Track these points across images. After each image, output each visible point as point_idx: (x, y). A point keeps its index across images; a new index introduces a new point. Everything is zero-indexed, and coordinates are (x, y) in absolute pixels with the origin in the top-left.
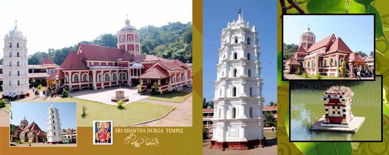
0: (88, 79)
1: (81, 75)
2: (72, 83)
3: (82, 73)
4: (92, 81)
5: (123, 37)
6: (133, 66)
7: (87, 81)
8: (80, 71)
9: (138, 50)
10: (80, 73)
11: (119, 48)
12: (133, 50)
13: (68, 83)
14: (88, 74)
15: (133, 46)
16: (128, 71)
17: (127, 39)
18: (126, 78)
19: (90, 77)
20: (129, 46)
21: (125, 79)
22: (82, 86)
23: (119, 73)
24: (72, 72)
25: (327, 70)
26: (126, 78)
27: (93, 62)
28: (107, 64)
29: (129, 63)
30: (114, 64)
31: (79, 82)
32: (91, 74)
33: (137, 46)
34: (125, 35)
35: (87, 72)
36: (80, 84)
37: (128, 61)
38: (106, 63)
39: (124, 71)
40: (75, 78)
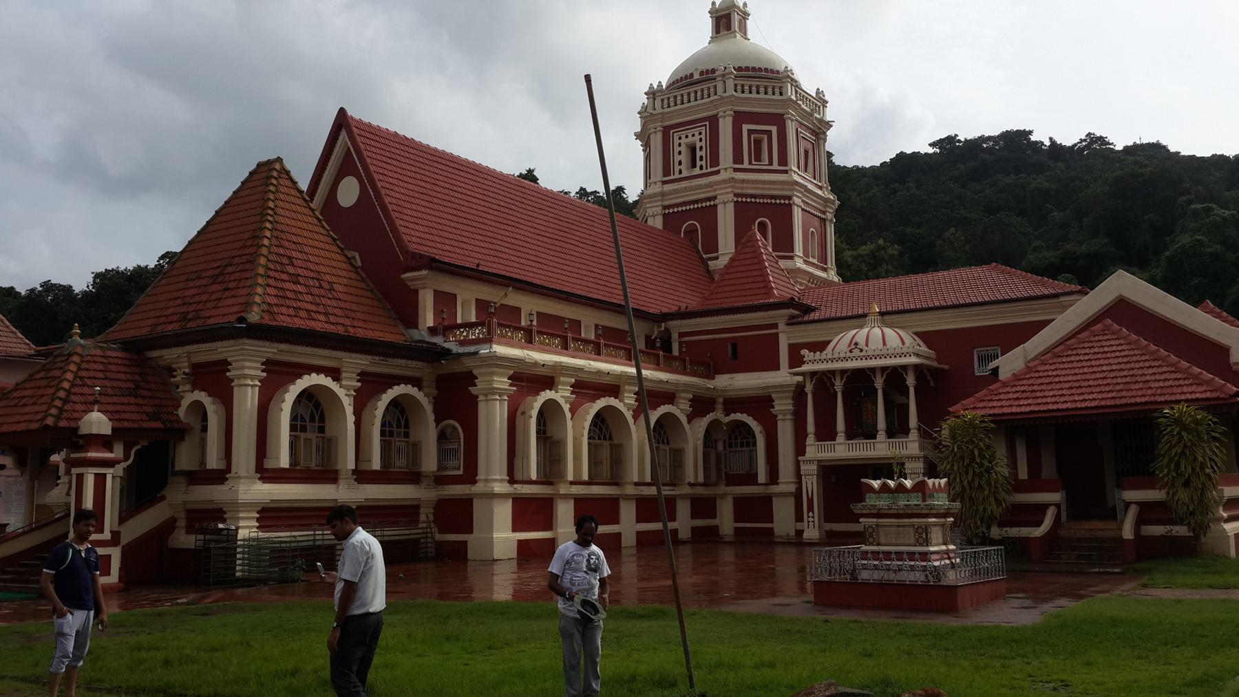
4: (470, 475)
5: (698, 136)
9: (823, 259)
11: (658, 223)
12: (784, 244)
13: (220, 476)
16: (783, 406)
17: (738, 158)
18: (762, 478)
19: (442, 437)
20: (747, 211)
21: (751, 479)
23: (703, 423)
24: (269, 365)
26: (762, 478)
27: (467, 297)
28: (588, 333)
31: (328, 475)
32: (457, 397)
34: (713, 121)
38: (576, 325)
39: (734, 403)
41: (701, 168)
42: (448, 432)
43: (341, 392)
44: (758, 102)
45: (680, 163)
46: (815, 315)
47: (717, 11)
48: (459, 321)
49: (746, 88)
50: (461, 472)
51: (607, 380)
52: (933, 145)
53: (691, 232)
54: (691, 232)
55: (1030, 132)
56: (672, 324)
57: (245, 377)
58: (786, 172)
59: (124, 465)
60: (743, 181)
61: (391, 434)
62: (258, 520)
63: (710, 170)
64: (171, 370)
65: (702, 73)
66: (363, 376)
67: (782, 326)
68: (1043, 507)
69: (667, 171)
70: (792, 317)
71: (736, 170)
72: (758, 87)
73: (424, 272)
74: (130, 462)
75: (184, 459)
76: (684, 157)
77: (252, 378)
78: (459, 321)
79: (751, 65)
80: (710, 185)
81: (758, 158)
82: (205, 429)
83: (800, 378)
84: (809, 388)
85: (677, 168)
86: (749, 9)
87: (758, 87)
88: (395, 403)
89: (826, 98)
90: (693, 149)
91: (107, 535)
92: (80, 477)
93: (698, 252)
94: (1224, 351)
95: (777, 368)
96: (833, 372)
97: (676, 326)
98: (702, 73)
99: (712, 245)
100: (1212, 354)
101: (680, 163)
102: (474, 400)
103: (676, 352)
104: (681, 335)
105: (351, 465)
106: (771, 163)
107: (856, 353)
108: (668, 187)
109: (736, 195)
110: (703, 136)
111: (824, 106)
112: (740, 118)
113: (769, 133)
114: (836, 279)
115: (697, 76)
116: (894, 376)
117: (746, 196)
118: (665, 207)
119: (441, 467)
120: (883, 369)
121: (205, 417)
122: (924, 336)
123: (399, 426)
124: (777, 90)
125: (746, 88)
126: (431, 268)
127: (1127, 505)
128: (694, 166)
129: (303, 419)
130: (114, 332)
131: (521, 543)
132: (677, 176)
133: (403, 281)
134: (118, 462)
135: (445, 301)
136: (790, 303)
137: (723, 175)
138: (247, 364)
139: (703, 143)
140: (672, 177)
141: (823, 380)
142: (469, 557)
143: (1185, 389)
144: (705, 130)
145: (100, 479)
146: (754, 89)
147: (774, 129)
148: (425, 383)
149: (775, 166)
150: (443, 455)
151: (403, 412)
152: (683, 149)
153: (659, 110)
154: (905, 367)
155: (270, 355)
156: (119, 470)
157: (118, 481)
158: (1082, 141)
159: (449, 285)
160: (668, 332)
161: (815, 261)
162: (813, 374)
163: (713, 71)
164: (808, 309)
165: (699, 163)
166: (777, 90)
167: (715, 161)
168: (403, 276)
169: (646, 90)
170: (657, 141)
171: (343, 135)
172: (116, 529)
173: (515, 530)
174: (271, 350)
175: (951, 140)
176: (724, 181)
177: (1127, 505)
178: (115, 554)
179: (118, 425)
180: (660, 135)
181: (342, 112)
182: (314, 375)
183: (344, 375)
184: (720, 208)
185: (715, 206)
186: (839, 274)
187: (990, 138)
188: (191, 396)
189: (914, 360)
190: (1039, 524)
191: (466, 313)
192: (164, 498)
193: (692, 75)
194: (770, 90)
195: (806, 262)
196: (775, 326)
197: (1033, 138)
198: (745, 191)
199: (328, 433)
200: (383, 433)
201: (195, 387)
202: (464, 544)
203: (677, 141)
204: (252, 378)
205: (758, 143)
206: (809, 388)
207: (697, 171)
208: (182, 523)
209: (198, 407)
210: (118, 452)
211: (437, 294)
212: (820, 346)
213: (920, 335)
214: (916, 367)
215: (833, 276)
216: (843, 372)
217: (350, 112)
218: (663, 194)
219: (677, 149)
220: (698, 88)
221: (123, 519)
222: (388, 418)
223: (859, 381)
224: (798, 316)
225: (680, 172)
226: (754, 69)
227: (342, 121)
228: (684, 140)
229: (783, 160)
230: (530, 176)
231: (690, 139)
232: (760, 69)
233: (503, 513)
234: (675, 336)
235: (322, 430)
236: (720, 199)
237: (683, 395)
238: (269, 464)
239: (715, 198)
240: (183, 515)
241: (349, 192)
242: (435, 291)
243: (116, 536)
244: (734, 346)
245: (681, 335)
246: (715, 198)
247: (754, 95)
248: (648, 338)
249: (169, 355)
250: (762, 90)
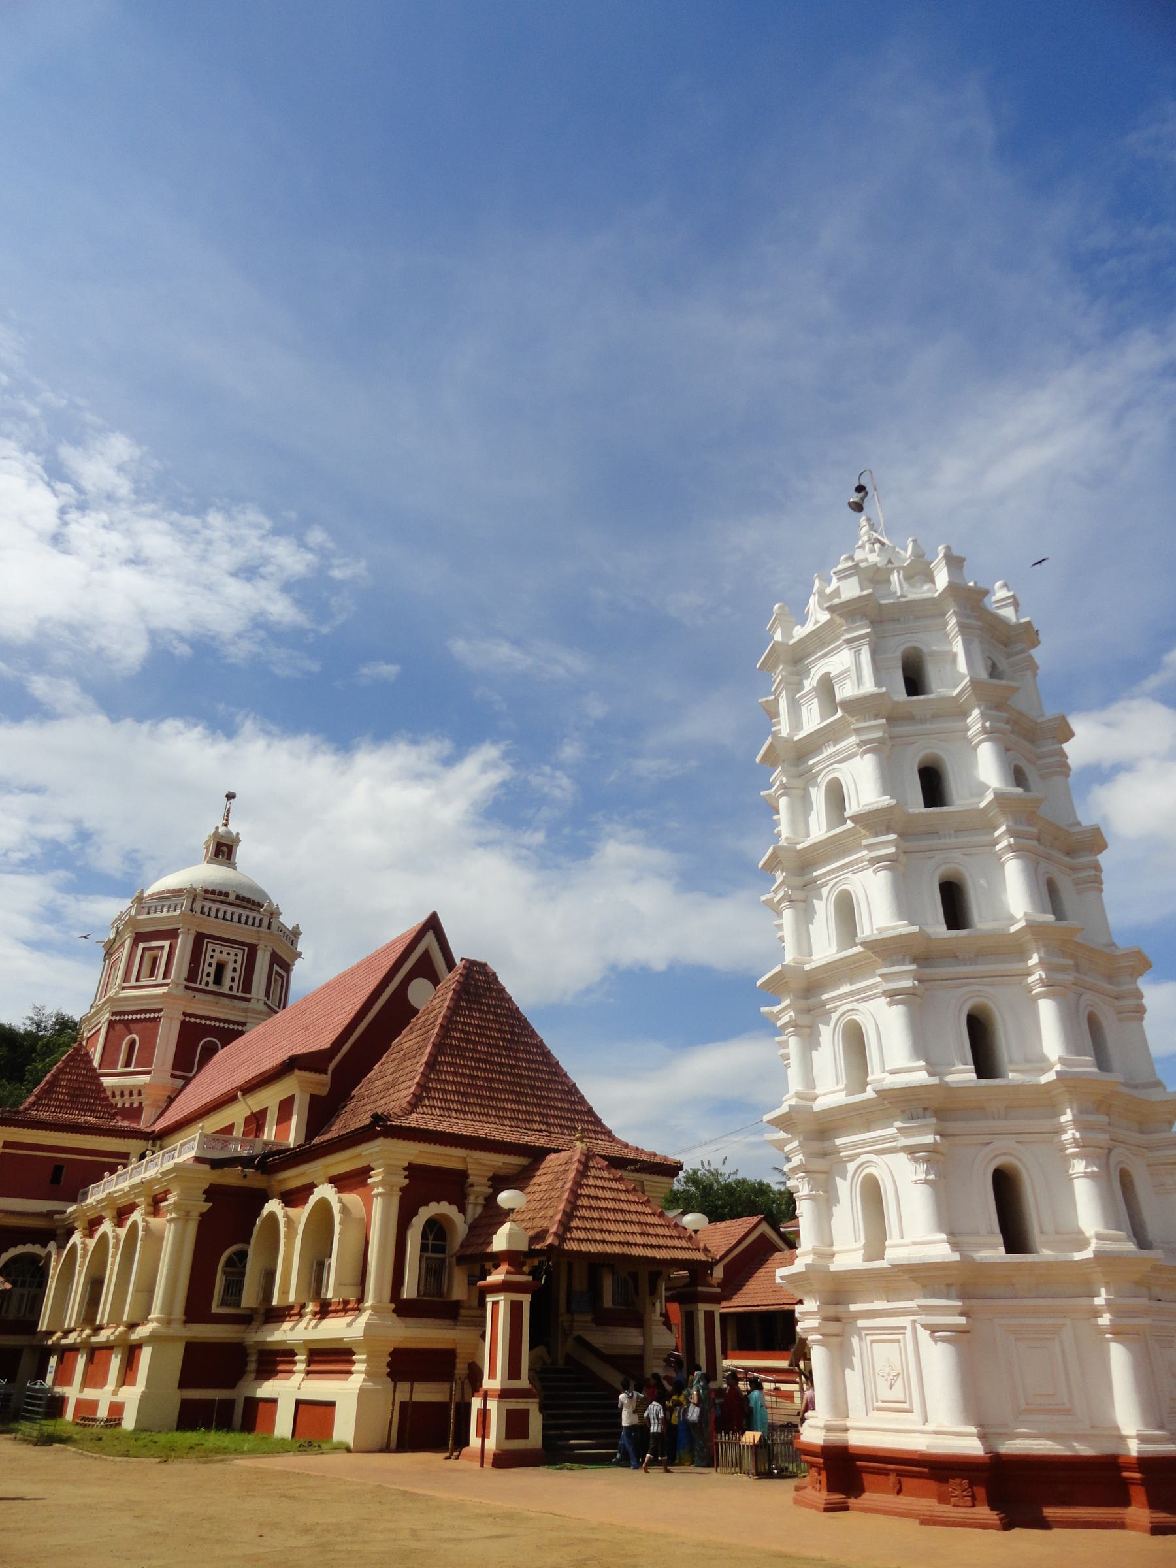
5: (233, 960)
25: (274, 1361)
41: (231, 988)
45: (209, 975)
63: (240, 994)
85: (205, 979)
90: (220, 968)
98: (238, 897)
110: (239, 959)
115: (232, 898)
118: (185, 1014)
132: (203, 987)
140: (197, 986)
165: (227, 982)
193: (227, 894)
203: (209, 953)
219: (208, 960)
220: (230, 909)
225: (207, 984)
231: (224, 957)
246: (244, 1024)
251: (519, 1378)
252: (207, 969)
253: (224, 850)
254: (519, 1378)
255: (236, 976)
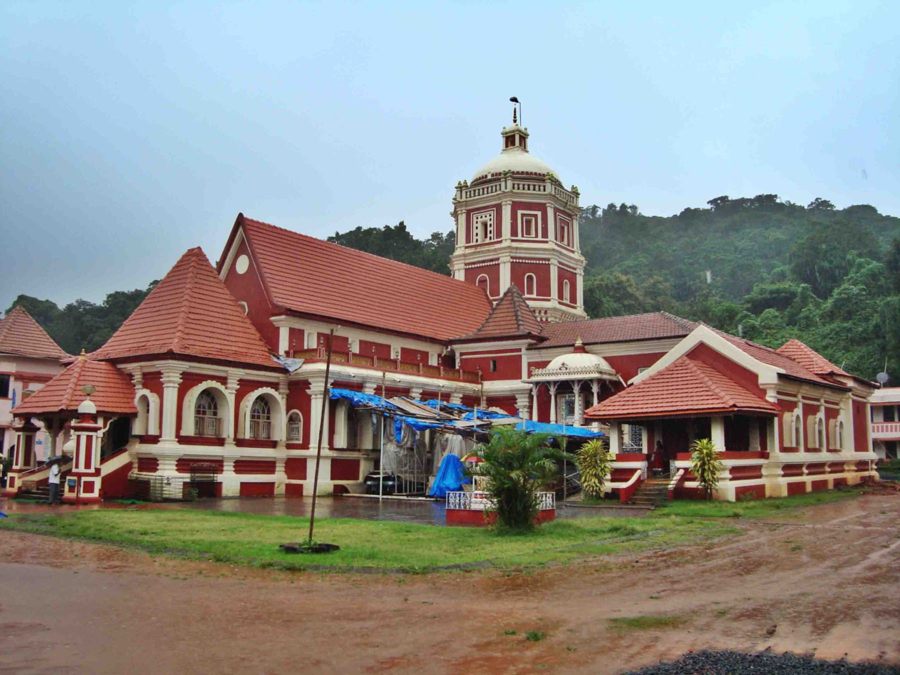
0: (280, 431)
1: (240, 396)
2: (183, 440)
3: (246, 386)
4: (305, 445)
5: (489, 217)
6: (550, 366)
7: (274, 445)
8: (235, 375)
9: (573, 299)
10: (234, 385)
11: (460, 276)
12: (544, 291)
13: (155, 440)
14: (280, 398)
15: (542, 269)
17: (514, 232)
19: (292, 420)
22: (242, 466)
24: (185, 375)
29: (526, 358)
30: (433, 361)
31: (221, 442)
33: (567, 275)
34: (499, 208)
35: (275, 386)
36: (230, 451)
37: (523, 343)
39: (493, 401)
40: (200, 411)
42: (294, 416)
43: (226, 392)
44: (529, 195)
45: (477, 235)
46: (546, 344)
47: (506, 133)
48: (306, 348)
49: (521, 186)
50: (301, 442)
51: (401, 385)
52: (710, 202)
53: (483, 281)
54: (483, 281)
55: (776, 196)
56: (455, 346)
57: (169, 382)
58: (547, 242)
59: (103, 431)
60: (517, 248)
61: (259, 417)
62: (177, 465)
64: (130, 376)
65: (493, 175)
66: (241, 382)
67: (524, 351)
68: (632, 471)
69: (468, 240)
70: (530, 345)
71: (513, 241)
72: (529, 185)
73: (283, 317)
74: (107, 429)
75: (137, 429)
76: (480, 231)
77: (174, 382)
78: (306, 348)
79: (525, 170)
80: (495, 250)
81: (528, 233)
82: (148, 411)
83: (531, 385)
84: (534, 393)
86: (529, 132)
87: (529, 185)
88: (261, 398)
89: (579, 191)
90: (485, 225)
91: (92, 470)
92: (79, 437)
93: (487, 296)
94: (755, 377)
95: (521, 378)
96: (549, 382)
97: (458, 348)
98: (493, 175)
99: (495, 292)
100: (747, 379)
101: (477, 235)
102: (308, 398)
103: (457, 367)
104: (462, 354)
105: (232, 436)
106: (537, 236)
107: (564, 370)
108: (468, 251)
109: (512, 258)
111: (577, 197)
112: (516, 206)
113: (536, 216)
114: (585, 314)
115: (489, 177)
116: (585, 386)
117: (520, 258)
118: (466, 264)
119: (288, 439)
120: (579, 381)
121: (148, 406)
122: (609, 360)
123: (263, 412)
124: (542, 188)
125: (521, 186)
126: (287, 315)
127: (678, 469)
128: (486, 237)
129: (204, 408)
130: (101, 352)
131: (335, 486)
132: (474, 244)
133: (271, 324)
134: (100, 429)
135: (296, 335)
136: (529, 336)
137: (505, 244)
138: (171, 374)
139: (492, 222)
140: (471, 244)
141: (543, 387)
142: (304, 494)
143: (710, 402)
144: (493, 213)
145: (89, 439)
146: (526, 187)
147: (539, 213)
148: (281, 386)
149: (540, 238)
150: (291, 430)
151: (266, 404)
152: (479, 225)
153: (464, 199)
154: (591, 380)
155: (185, 370)
156: (100, 433)
157: (100, 440)
158: (812, 204)
159: (298, 324)
160: (453, 352)
161: (568, 302)
162: (537, 383)
163: (500, 174)
164: (542, 339)
165: (489, 235)
166: (542, 188)
167: (499, 234)
168: (273, 318)
169: (457, 185)
170: (462, 218)
171: (241, 229)
172: (98, 467)
173: (332, 478)
174: (185, 366)
175: (724, 199)
176: (504, 248)
177: (678, 469)
178: (98, 482)
179: (101, 409)
180: (464, 216)
181: (241, 215)
182: (209, 381)
183: (229, 381)
184: (501, 266)
185: (498, 264)
186: (585, 310)
187: (750, 200)
188: (141, 392)
189: (596, 375)
190: (626, 480)
191: (311, 342)
192: (126, 450)
193: (486, 176)
194: (537, 187)
195: (560, 303)
196: (520, 350)
197: (778, 201)
198: (518, 255)
199: (218, 417)
200: (253, 417)
201: (145, 386)
202: (301, 486)
204: (174, 382)
205: (529, 223)
206: (534, 393)
207: (487, 241)
208: (136, 465)
209: (144, 398)
210: (100, 423)
211: (292, 332)
212: (544, 365)
213: (605, 358)
214: (601, 382)
215: (579, 310)
216: (555, 382)
217: (245, 216)
218: (464, 255)
219: (475, 225)
221: (103, 460)
222: (256, 407)
223: (565, 387)
224: (535, 344)
226: (527, 173)
227: (241, 221)
228: (479, 220)
229: (545, 234)
230: (402, 226)
231: (484, 219)
232: (531, 173)
233: (326, 468)
234: (457, 355)
235: (215, 414)
236: (501, 260)
237: (455, 395)
238: (183, 433)
239: (498, 259)
240: (136, 461)
241: (243, 265)
242: (290, 329)
243: (98, 472)
244: (495, 363)
245: (462, 354)
246: (498, 259)
247: (526, 191)
248: (439, 356)
249: (129, 367)
250: (532, 187)
251: (92, 491)
252: (492, 229)
253: (515, 139)
254: (92, 491)
255: (475, 231)
